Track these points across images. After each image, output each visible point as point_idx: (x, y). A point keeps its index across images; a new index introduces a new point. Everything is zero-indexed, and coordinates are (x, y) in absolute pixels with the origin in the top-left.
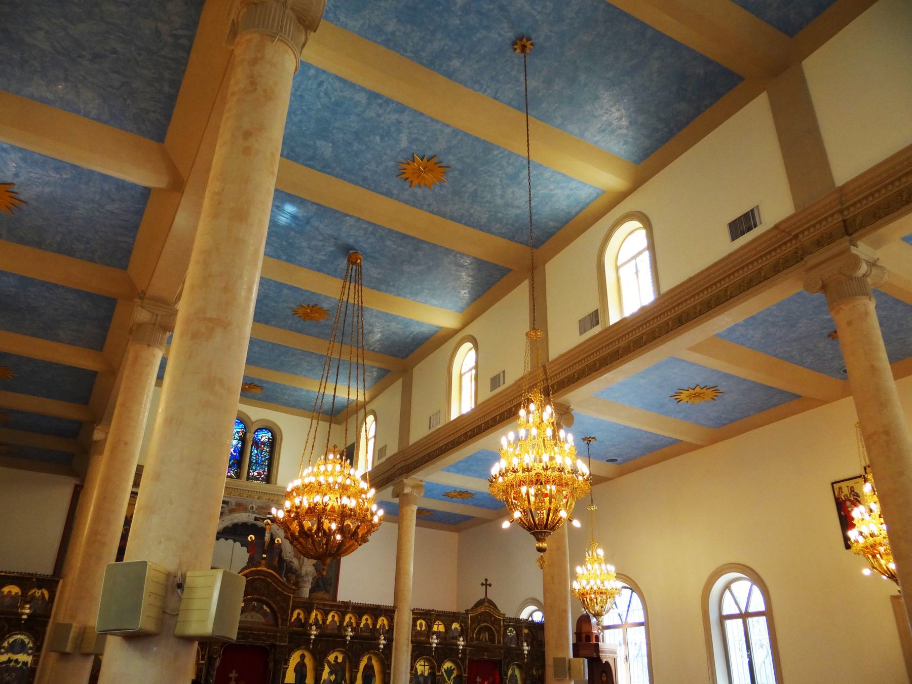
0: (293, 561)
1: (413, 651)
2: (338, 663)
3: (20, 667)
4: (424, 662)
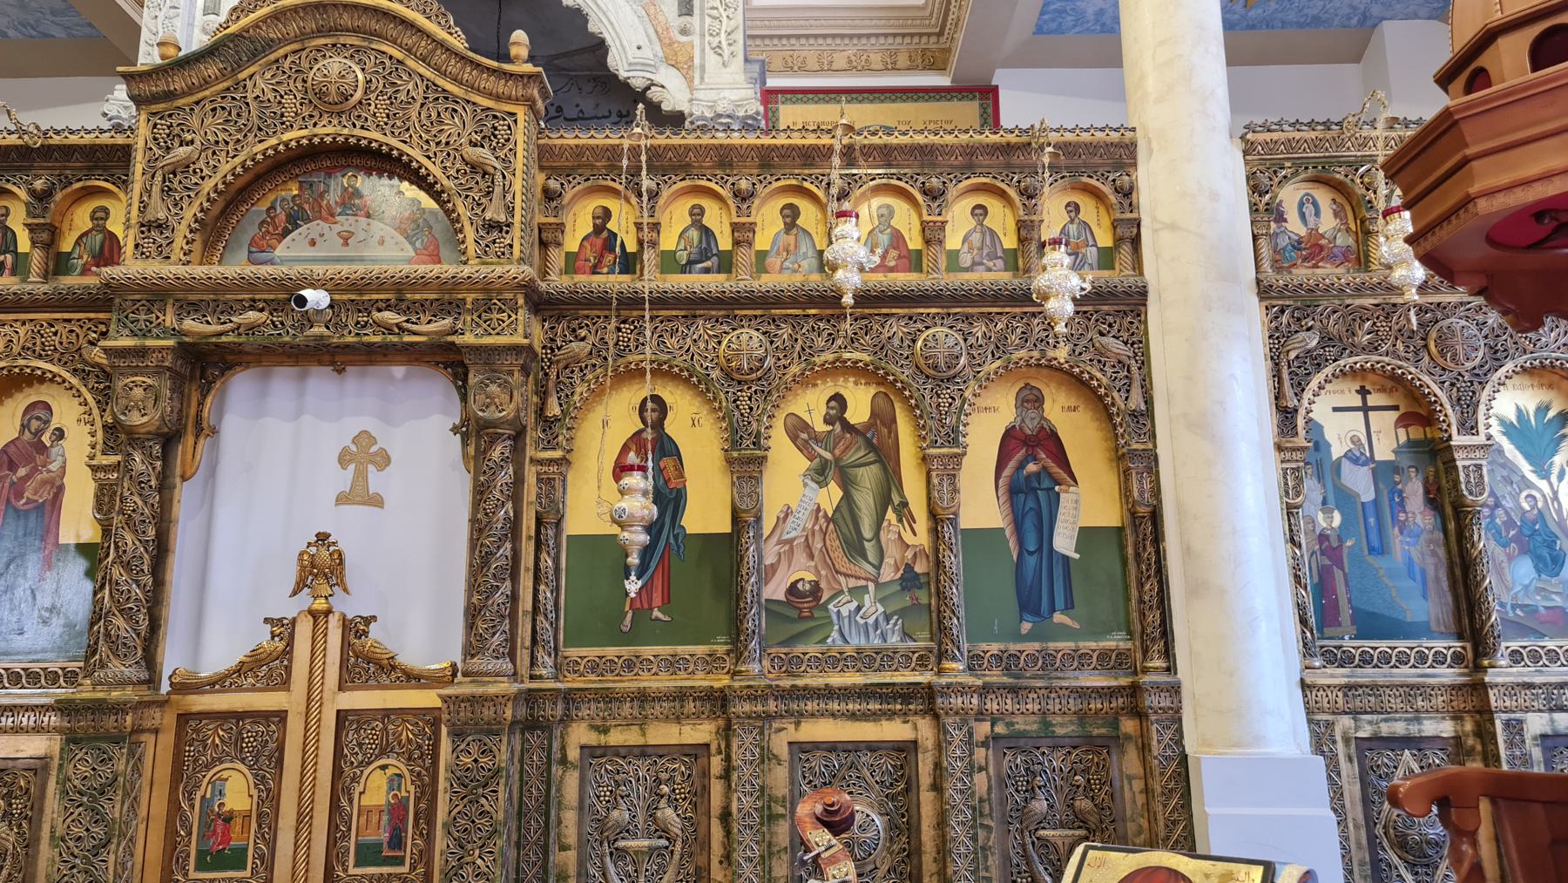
0: (657, 79)
2: (848, 427)
4: (1363, 392)
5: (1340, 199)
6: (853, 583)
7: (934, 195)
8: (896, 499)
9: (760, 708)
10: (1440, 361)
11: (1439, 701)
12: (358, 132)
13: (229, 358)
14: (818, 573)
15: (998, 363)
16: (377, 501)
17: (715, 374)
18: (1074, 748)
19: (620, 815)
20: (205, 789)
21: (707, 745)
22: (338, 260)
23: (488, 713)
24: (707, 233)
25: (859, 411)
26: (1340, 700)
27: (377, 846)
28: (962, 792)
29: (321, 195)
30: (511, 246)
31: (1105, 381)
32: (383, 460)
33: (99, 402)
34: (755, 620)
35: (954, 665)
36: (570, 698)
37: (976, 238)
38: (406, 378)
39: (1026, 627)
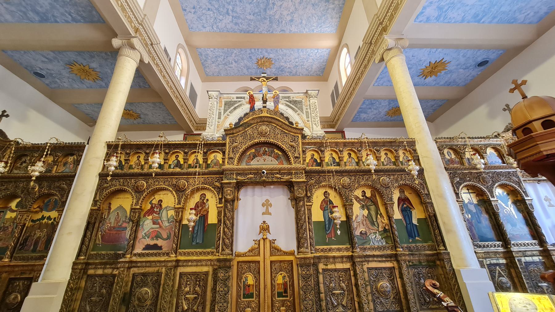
1: (452, 179)
2: (367, 197)
3: (52, 222)
5: (455, 152)
6: (374, 231)
7: (378, 151)
8: (379, 213)
9: (361, 260)
10: (484, 183)
11: (502, 255)
12: (268, 140)
13: (243, 184)
14: (366, 229)
15: (397, 184)
16: (270, 214)
17: (340, 187)
18: (427, 268)
19: (332, 285)
20: (244, 279)
21: (349, 269)
22: (263, 164)
23: (308, 261)
24: (333, 158)
25: (368, 194)
26: (483, 255)
27: (282, 293)
28: (408, 278)
29: (259, 152)
30: (300, 161)
31: (419, 187)
32: (271, 205)
33: (217, 194)
34: (356, 240)
35: (400, 249)
36: (319, 258)
37: (386, 159)
38: (273, 188)
39: (411, 240)
